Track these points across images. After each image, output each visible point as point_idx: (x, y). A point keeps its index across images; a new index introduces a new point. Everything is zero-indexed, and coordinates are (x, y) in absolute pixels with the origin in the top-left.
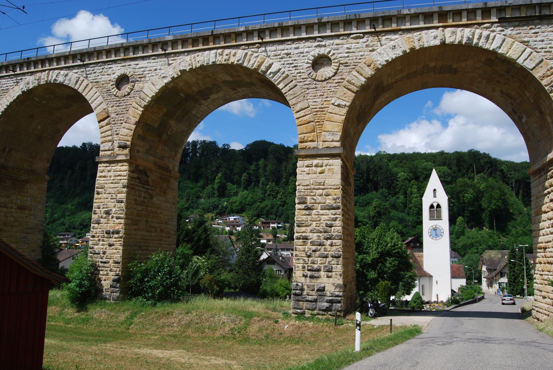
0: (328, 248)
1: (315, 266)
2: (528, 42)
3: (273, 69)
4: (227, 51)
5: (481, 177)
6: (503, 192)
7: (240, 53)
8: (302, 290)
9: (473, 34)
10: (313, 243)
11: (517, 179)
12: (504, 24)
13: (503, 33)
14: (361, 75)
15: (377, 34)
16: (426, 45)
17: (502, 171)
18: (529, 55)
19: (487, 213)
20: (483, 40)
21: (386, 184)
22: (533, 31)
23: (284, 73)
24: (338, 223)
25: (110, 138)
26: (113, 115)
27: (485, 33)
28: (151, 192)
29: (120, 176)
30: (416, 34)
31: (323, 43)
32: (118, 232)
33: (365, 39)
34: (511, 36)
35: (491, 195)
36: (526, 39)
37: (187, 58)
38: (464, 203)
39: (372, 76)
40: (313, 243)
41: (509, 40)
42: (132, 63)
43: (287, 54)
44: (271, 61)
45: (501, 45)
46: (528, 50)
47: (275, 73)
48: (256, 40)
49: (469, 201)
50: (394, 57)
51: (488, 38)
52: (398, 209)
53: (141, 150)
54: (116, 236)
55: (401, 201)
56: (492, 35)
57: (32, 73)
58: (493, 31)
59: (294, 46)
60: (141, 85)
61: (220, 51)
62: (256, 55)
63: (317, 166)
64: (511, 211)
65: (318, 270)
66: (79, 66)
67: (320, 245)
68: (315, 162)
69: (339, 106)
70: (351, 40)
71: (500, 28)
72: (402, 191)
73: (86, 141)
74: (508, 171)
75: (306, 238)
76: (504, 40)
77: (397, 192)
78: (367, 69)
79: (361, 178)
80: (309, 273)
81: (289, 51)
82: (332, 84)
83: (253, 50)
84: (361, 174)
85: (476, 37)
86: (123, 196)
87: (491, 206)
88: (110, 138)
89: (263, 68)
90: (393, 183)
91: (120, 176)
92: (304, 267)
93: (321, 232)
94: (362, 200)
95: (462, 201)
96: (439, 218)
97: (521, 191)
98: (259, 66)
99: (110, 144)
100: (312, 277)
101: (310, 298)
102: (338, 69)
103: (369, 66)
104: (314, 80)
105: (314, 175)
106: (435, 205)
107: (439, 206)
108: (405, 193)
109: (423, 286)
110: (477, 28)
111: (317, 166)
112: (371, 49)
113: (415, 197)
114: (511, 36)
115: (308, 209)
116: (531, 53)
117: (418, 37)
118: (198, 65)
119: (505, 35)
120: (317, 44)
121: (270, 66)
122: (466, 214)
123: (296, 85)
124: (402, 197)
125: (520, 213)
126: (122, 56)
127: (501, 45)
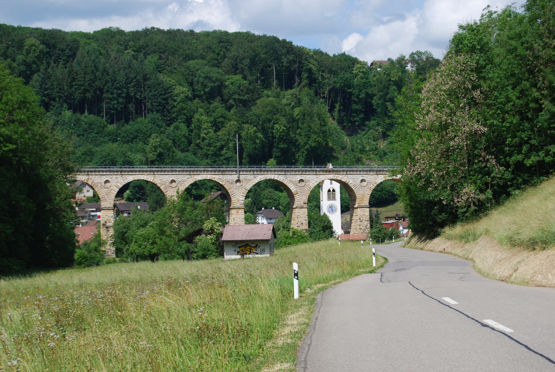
4: (336, 175)
5: (292, 96)
6: (324, 120)
11: (334, 87)
15: (377, 174)
17: (310, 71)
19: (303, 152)
21: (158, 106)
24: (369, 225)
26: (299, 193)
35: (310, 127)
37: (324, 176)
38: (274, 137)
48: (345, 173)
49: (280, 135)
52: (179, 146)
55: (183, 133)
57: (262, 174)
64: (330, 145)
66: (283, 174)
68: (363, 209)
72: (182, 118)
74: (319, 71)
77: (174, 118)
79: (119, 95)
82: (365, 188)
84: (118, 89)
87: (310, 142)
90: (168, 103)
94: (125, 132)
95: (271, 135)
96: (334, 198)
97: (337, 105)
106: (331, 190)
107: (334, 190)
108: (188, 121)
113: (205, 129)
115: (361, 221)
122: (275, 154)
124: (183, 127)
125: (343, 148)
126: (300, 173)
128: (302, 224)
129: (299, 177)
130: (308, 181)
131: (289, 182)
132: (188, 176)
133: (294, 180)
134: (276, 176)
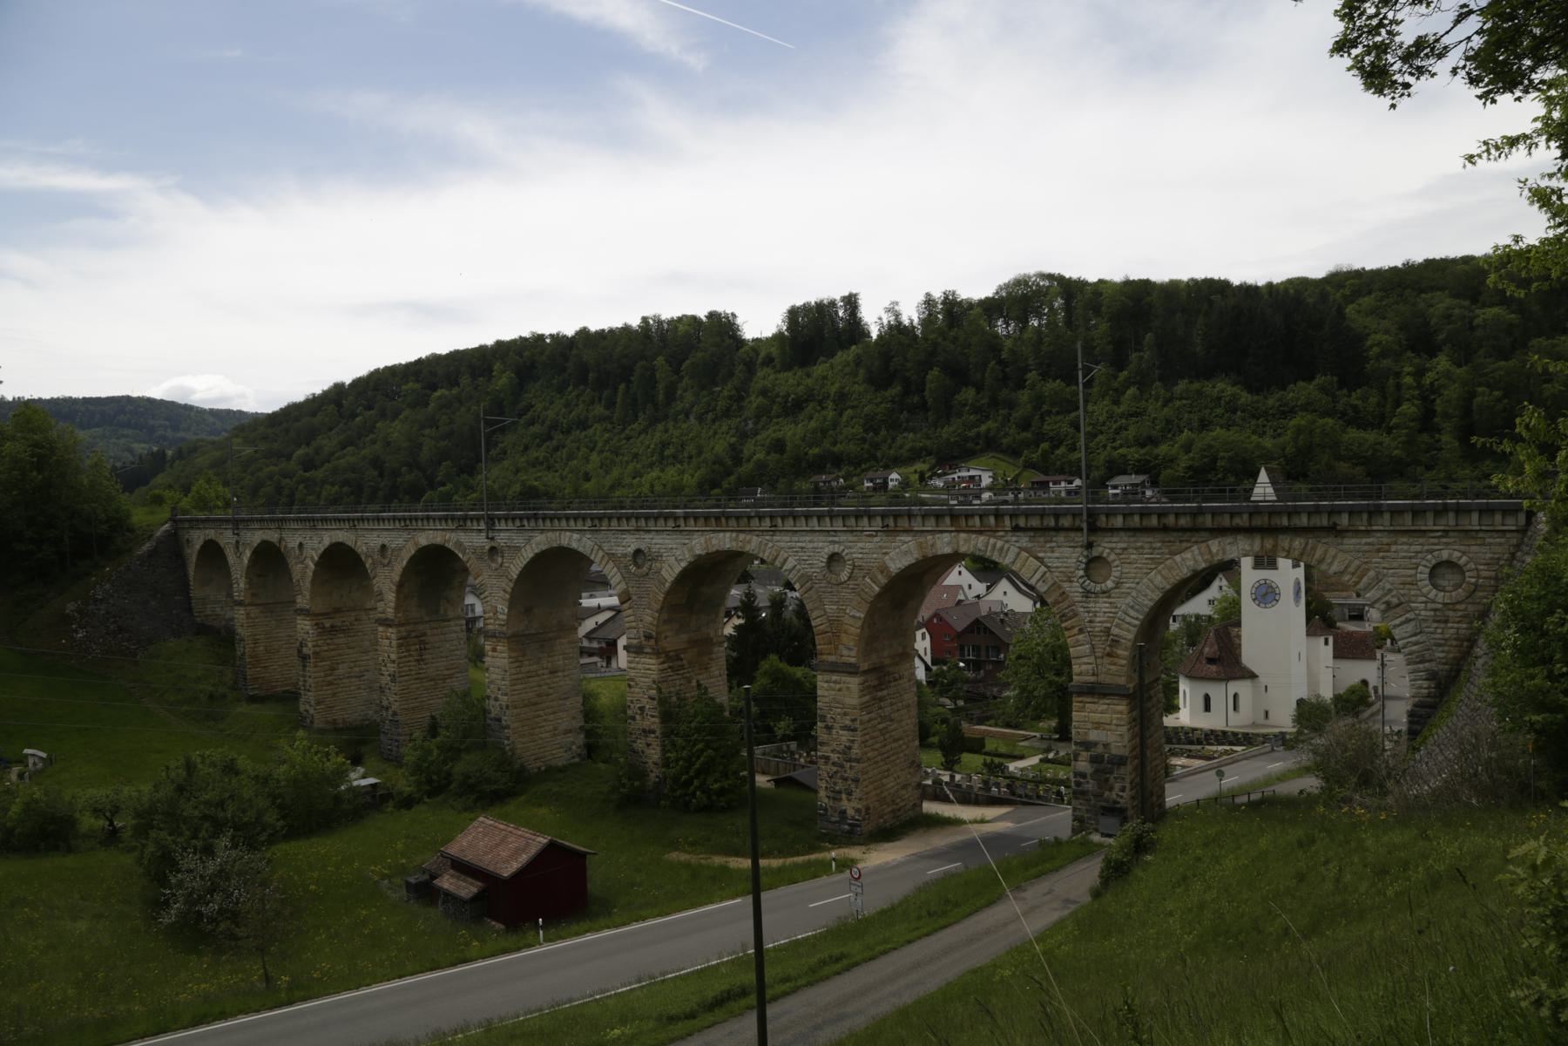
0: (849, 771)
1: (837, 788)
2: (1043, 558)
3: (788, 565)
4: (742, 536)
7: (755, 540)
8: (826, 810)
9: (988, 543)
10: (834, 764)
12: (1019, 534)
13: (1018, 545)
14: (874, 582)
16: (939, 552)
18: (1043, 576)
20: (996, 553)
22: (1048, 545)
23: (799, 570)
25: (634, 624)
26: (634, 598)
27: (999, 544)
28: (688, 675)
29: (649, 669)
30: (930, 537)
31: (836, 539)
32: (653, 732)
33: (876, 539)
34: (1026, 550)
36: (1040, 555)
39: (886, 585)
40: (834, 764)
41: (1024, 554)
42: (646, 536)
43: (802, 548)
44: (786, 555)
45: (1015, 560)
46: (1043, 569)
47: (791, 571)
50: (907, 564)
51: (1002, 549)
53: (669, 634)
54: (653, 735)
56: (1007, 546)
58: (1007, 542)
59: (808, 539)
60: (658, 565)
61: (734, 535)
62: (770, 544)
63: (835, 682)
65: (840, 792)
67: (842, 766)
68: (834, 678)
69: (853, 617)
70: (864, 538)
71: (1014, 539)
73: (649, 313)
75: (827, 758)
76: (1018, 554)
78: (880, 576)
80: (832, 795)
81: (803, 545)
83: (767, 538)
85: (989, 548)
86: (653, 692)
88: (634, 624)
89: (778, 563)
91: (649, 669)
92: (826, 788)
93: (839, 753)
98: (776, 558)
99: (635, 631)
100: (834, 799)
101: (833, 819)
102: (852, 572)
103: (882, 572)
104: (829, 583)
105: (833, 693)
109: (1236, 696)
110: (990, 536)
111: (835, 682)
112: (884, 551)
114: (1026, 550)
116: (1045, 573)
117: (931, 542)
118: (714, 550)
119: (1019, 548)
120: (831, 539)
121: (786, 560)
123: (811, 588)
127: (1015, 560)
128: (642, 709)
129: (631, 543)
130: (657, 558)
131: (606, 558)
132: (405, 535)
133: (620, 551)
134: (576, 536)
